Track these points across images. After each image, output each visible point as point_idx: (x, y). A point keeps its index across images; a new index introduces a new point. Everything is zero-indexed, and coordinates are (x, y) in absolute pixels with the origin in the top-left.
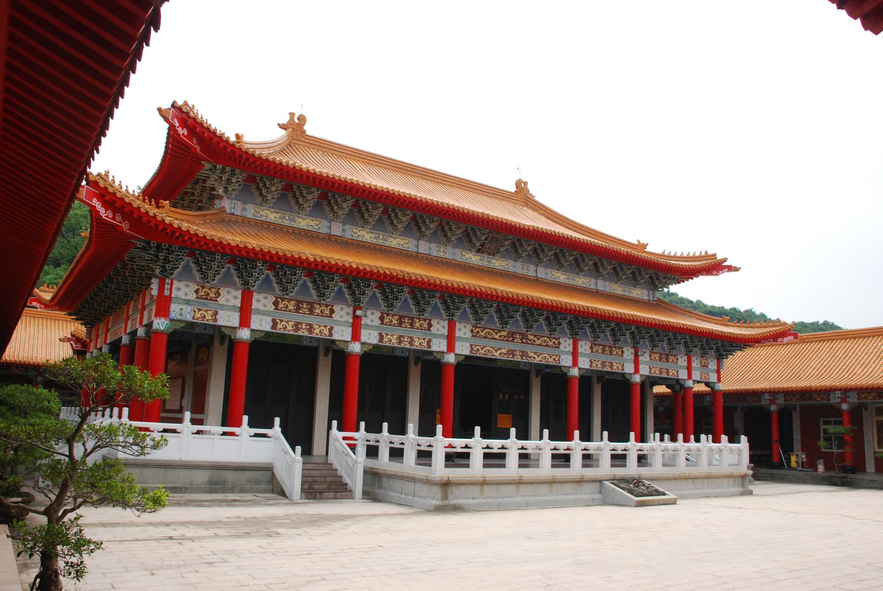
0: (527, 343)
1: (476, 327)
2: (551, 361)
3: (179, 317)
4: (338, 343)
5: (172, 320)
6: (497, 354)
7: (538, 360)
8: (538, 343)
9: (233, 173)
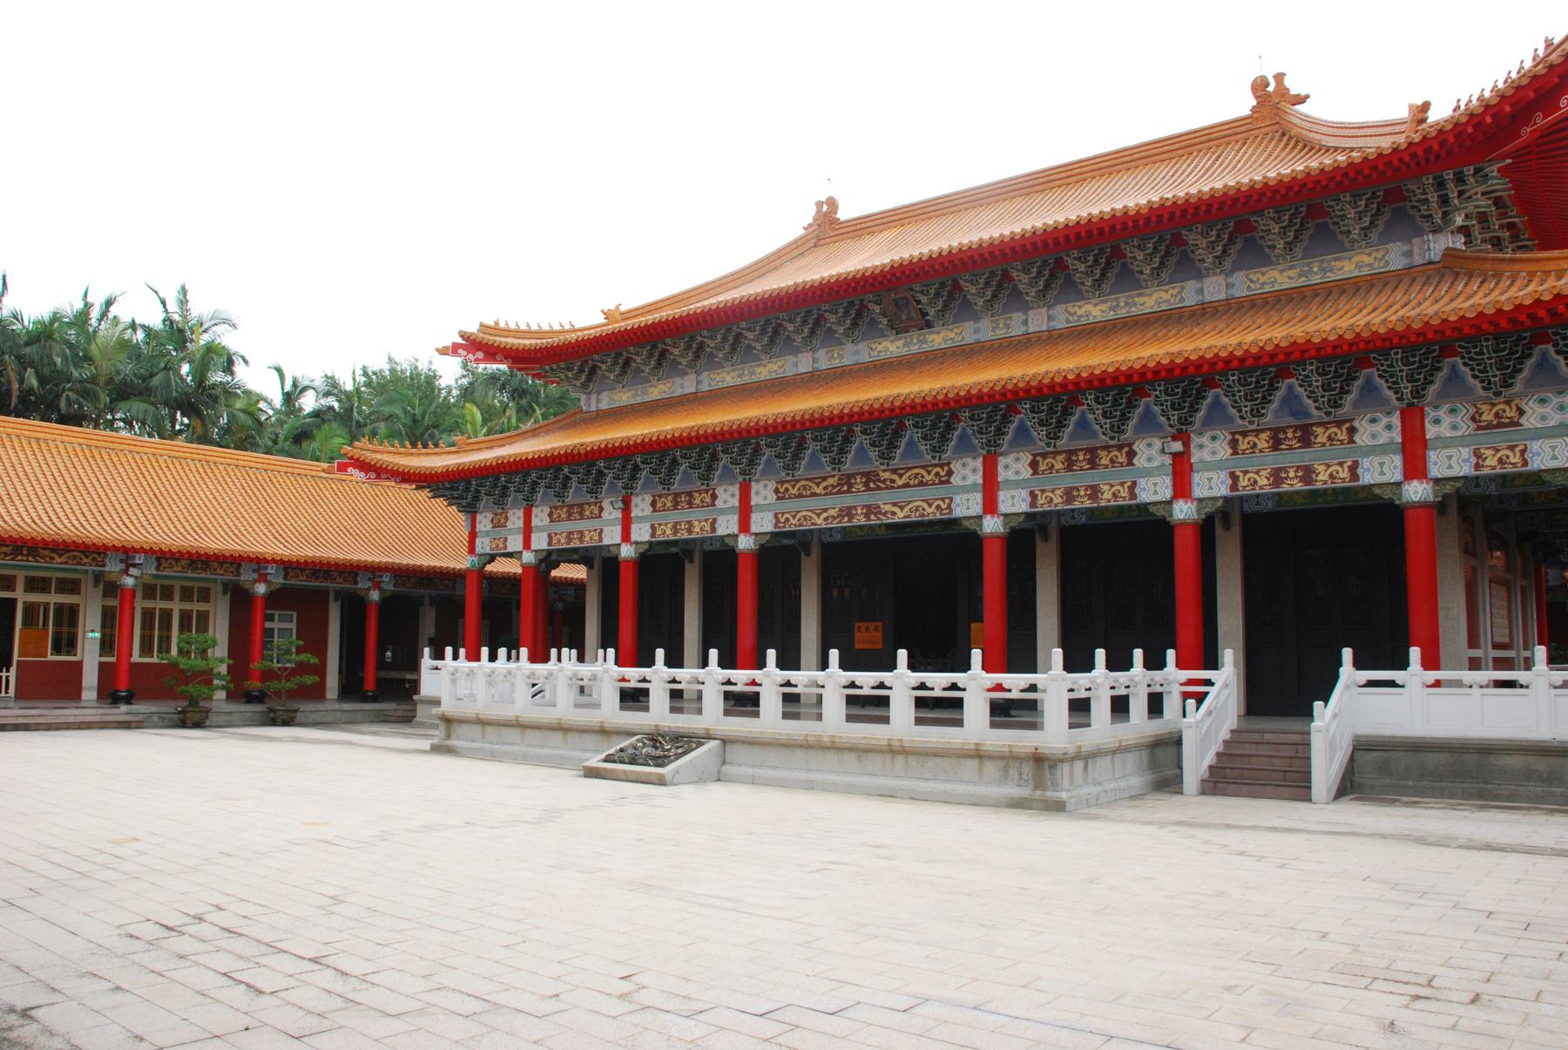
0: (879, 488)
1: (783, 483)
2: (931, 513)
6: (819, 521)
7: (900, 516)
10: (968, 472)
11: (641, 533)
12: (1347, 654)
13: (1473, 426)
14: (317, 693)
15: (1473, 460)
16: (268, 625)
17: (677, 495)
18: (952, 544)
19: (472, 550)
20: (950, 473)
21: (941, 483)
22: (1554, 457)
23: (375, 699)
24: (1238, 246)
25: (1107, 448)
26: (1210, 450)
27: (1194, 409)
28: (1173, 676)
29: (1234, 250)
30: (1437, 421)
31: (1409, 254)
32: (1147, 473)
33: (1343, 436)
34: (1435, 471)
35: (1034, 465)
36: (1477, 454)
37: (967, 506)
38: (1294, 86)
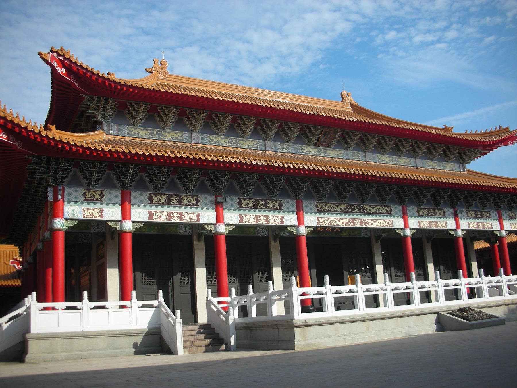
1: (320, 203)
3: (72, 217)
5: (67, 219)
8: (373, 211)
9: (106, 102)
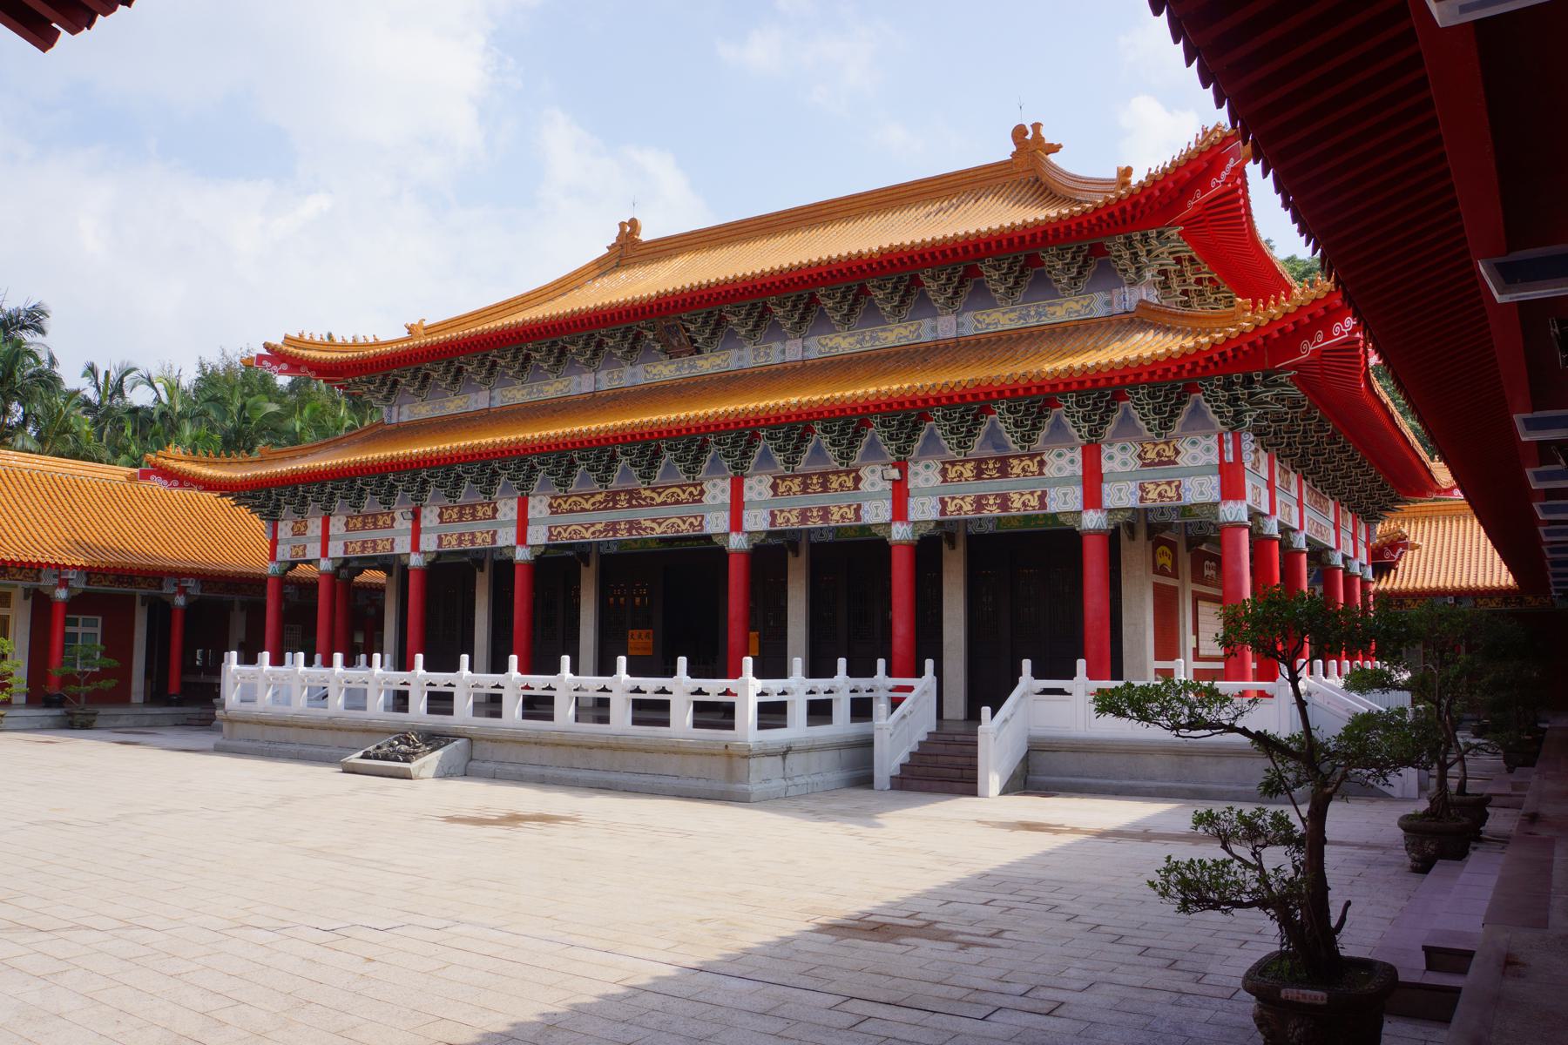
1: (556, 498)
2: (685, 530)
4: (715, 540)
7: (659, 531)
8: (659, 500)
10: (717, 491)
11: (429, 543)
12: (1027, 664)
13: (1140, 463)
14: (121, 696)
15: (1139, 493)
16: (69, 629)
17: (462, 507)
18: (696, 559)
19: (273, 557)
20: (702, 492)
21: (695, 501)
22: (1202, 493)
23: (179, 703)
24: (969, 289)
25: (837, 473)
26: (924, 476)
27: (910, 439)
28: (882, 681)
29: (964, 292)
30: (1111, 458)
31: (1109, 303)
32: (871, 497)
33: (1034, 468)
34: (1108, 502)
35: (774, 487)
36: (1142, 488)
37: (716, 523)
38: (1049, 137)
